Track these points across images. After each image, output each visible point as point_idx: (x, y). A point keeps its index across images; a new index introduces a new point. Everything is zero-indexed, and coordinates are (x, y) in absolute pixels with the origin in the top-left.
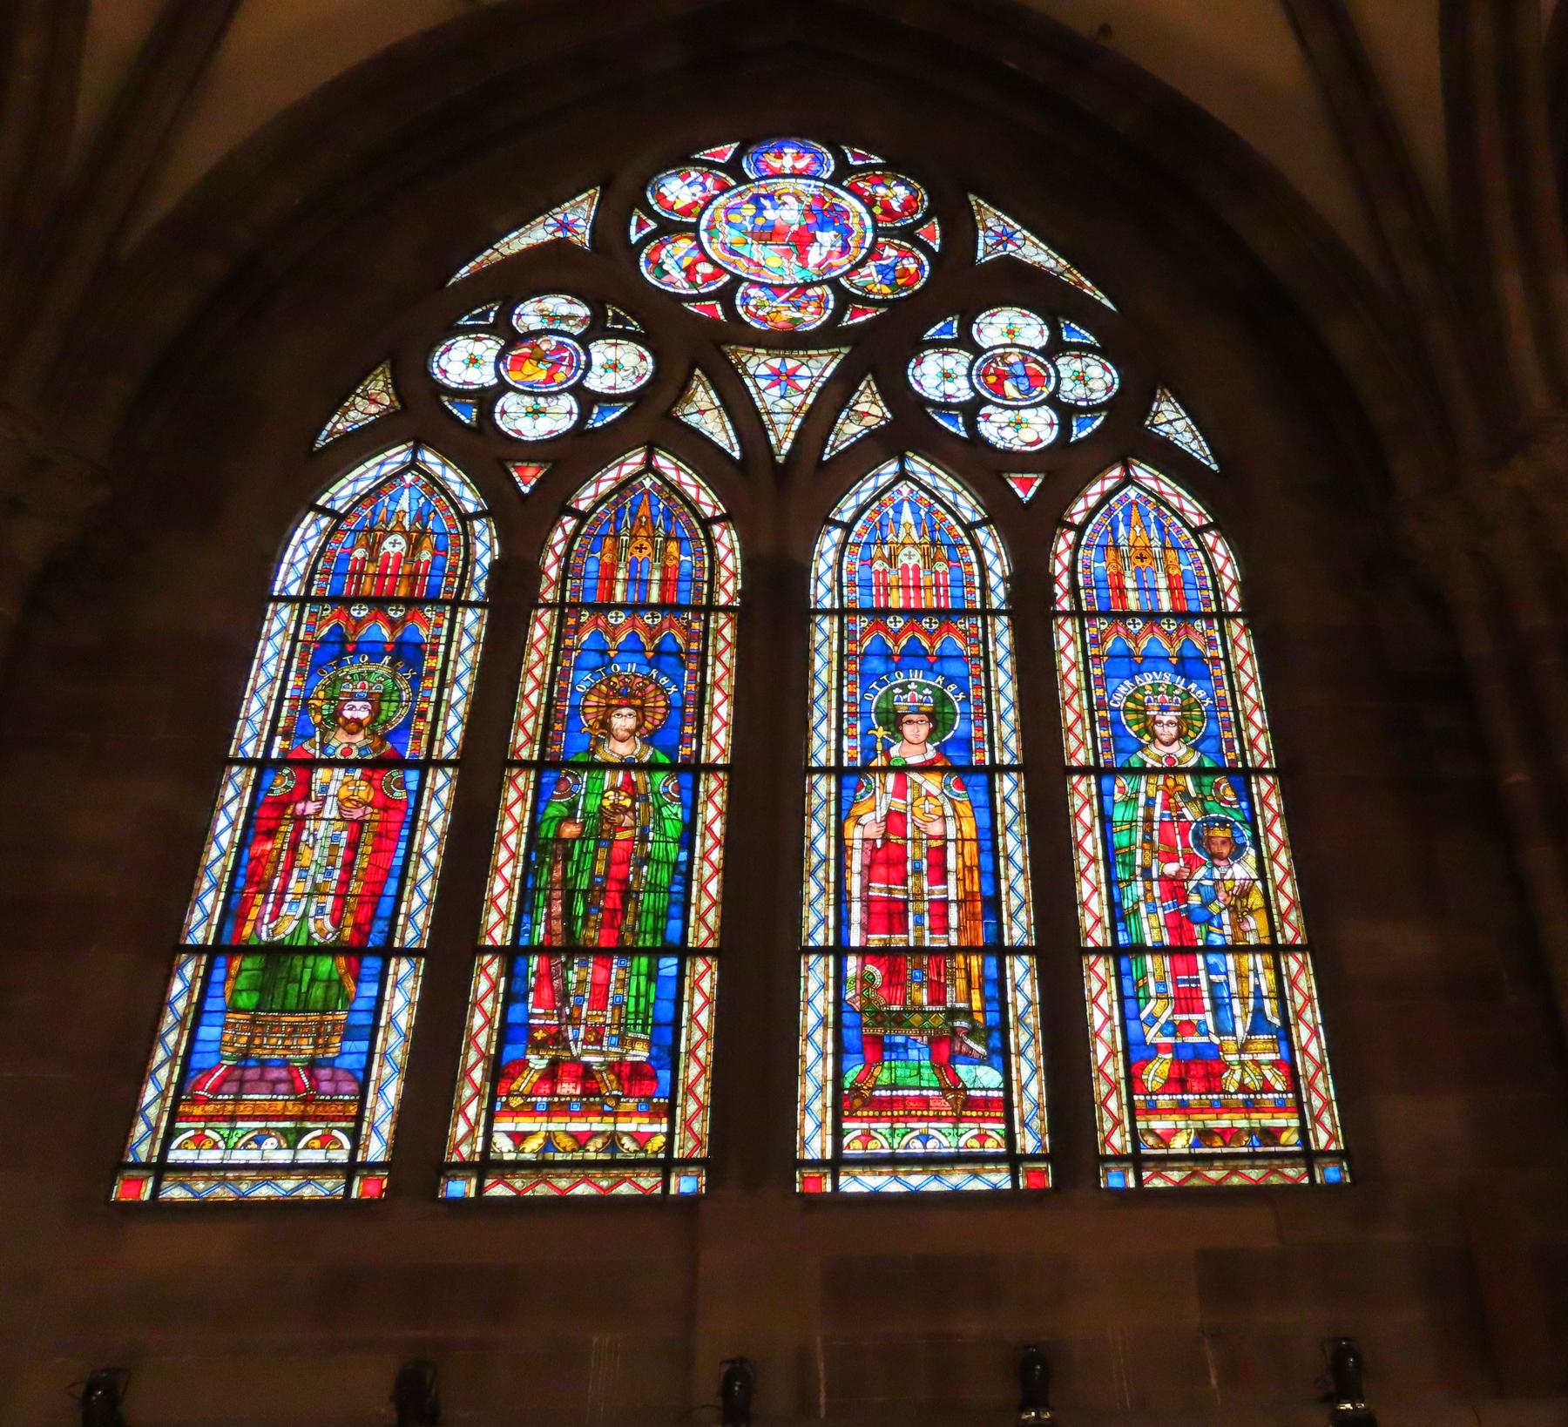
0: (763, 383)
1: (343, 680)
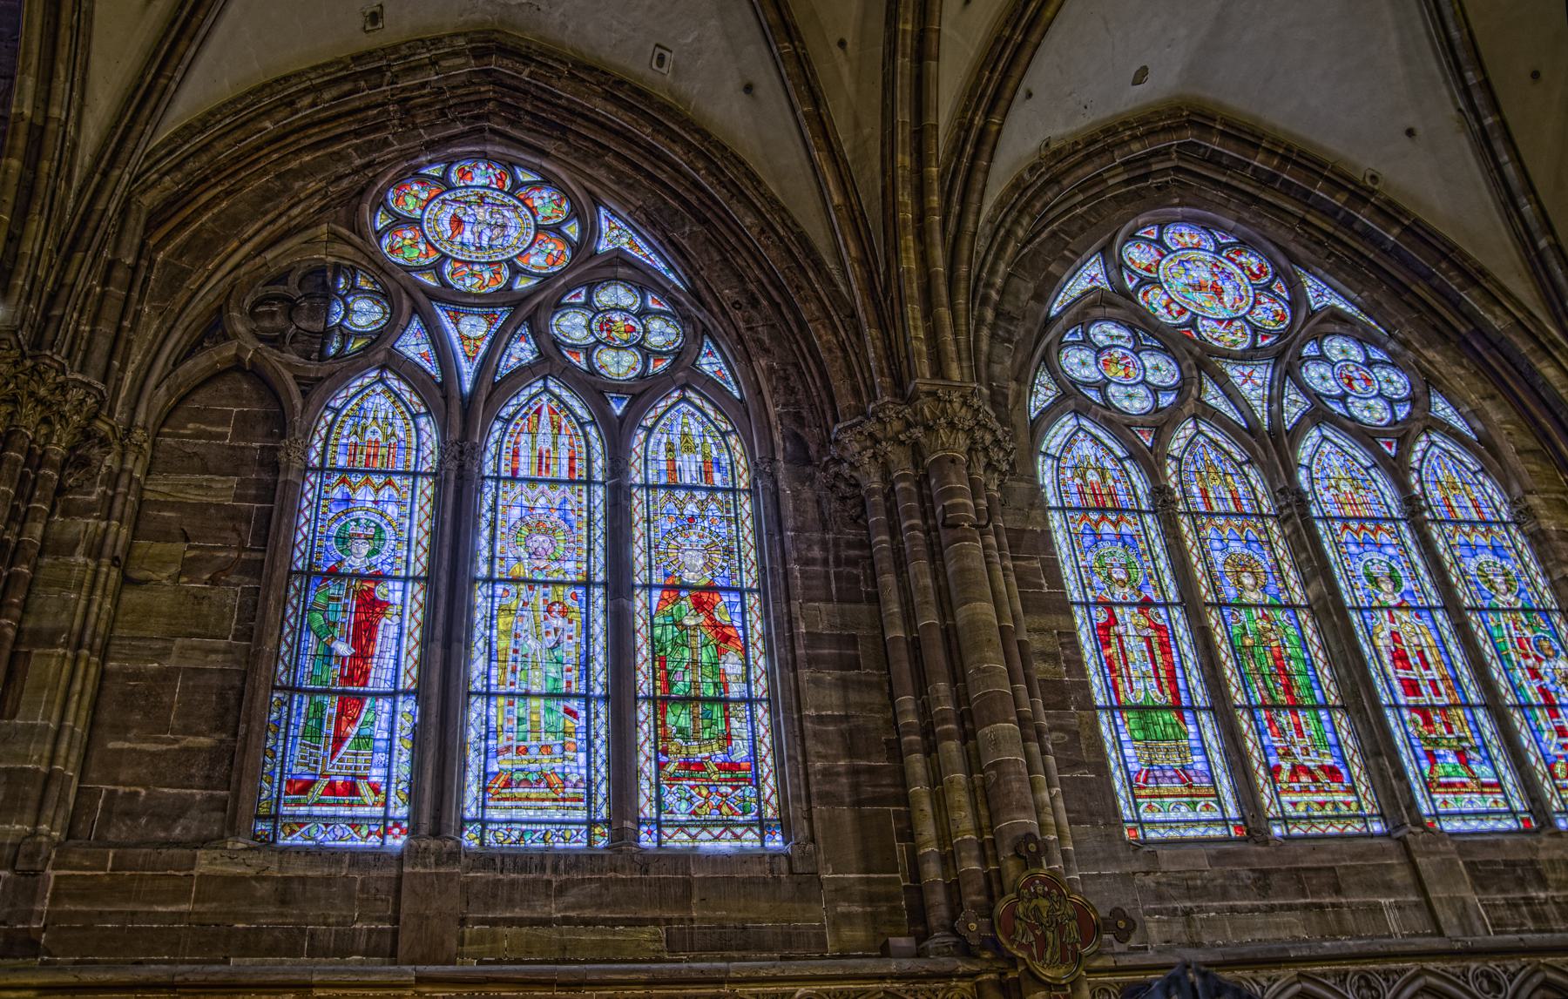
0: (1239, 381)
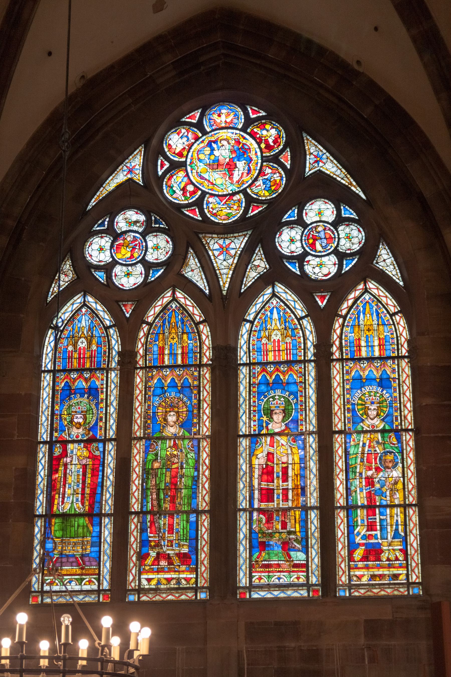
0: (216, 253)
1: (72, 406)
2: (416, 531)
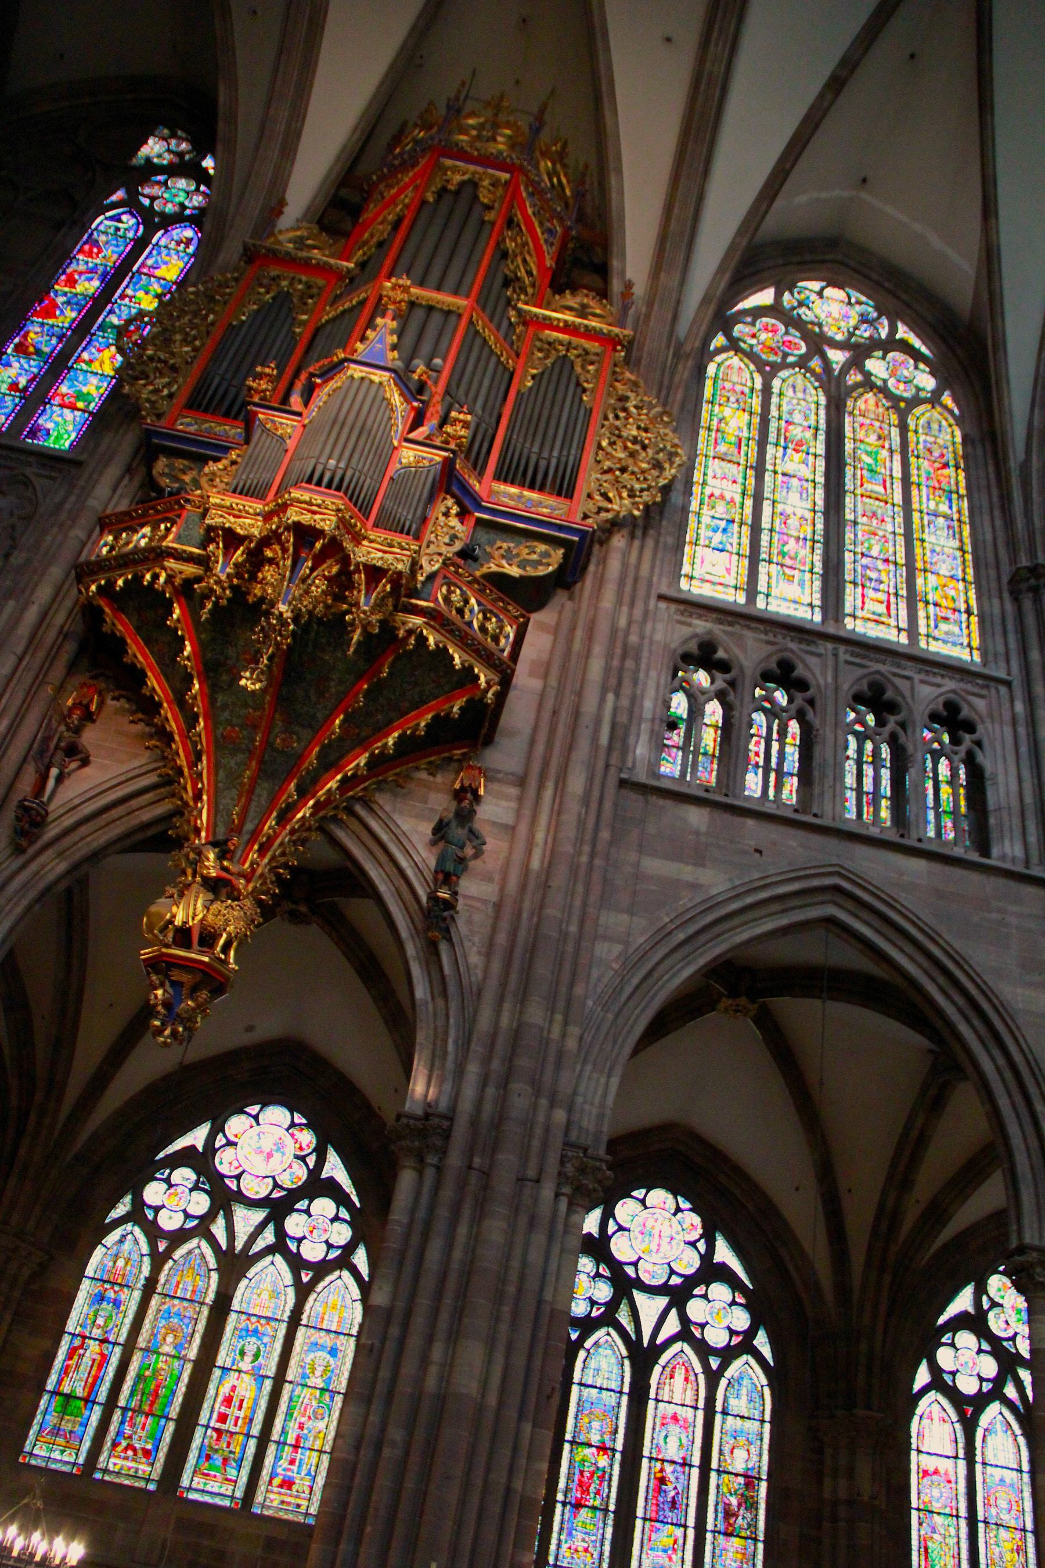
2: (324, 1473)
